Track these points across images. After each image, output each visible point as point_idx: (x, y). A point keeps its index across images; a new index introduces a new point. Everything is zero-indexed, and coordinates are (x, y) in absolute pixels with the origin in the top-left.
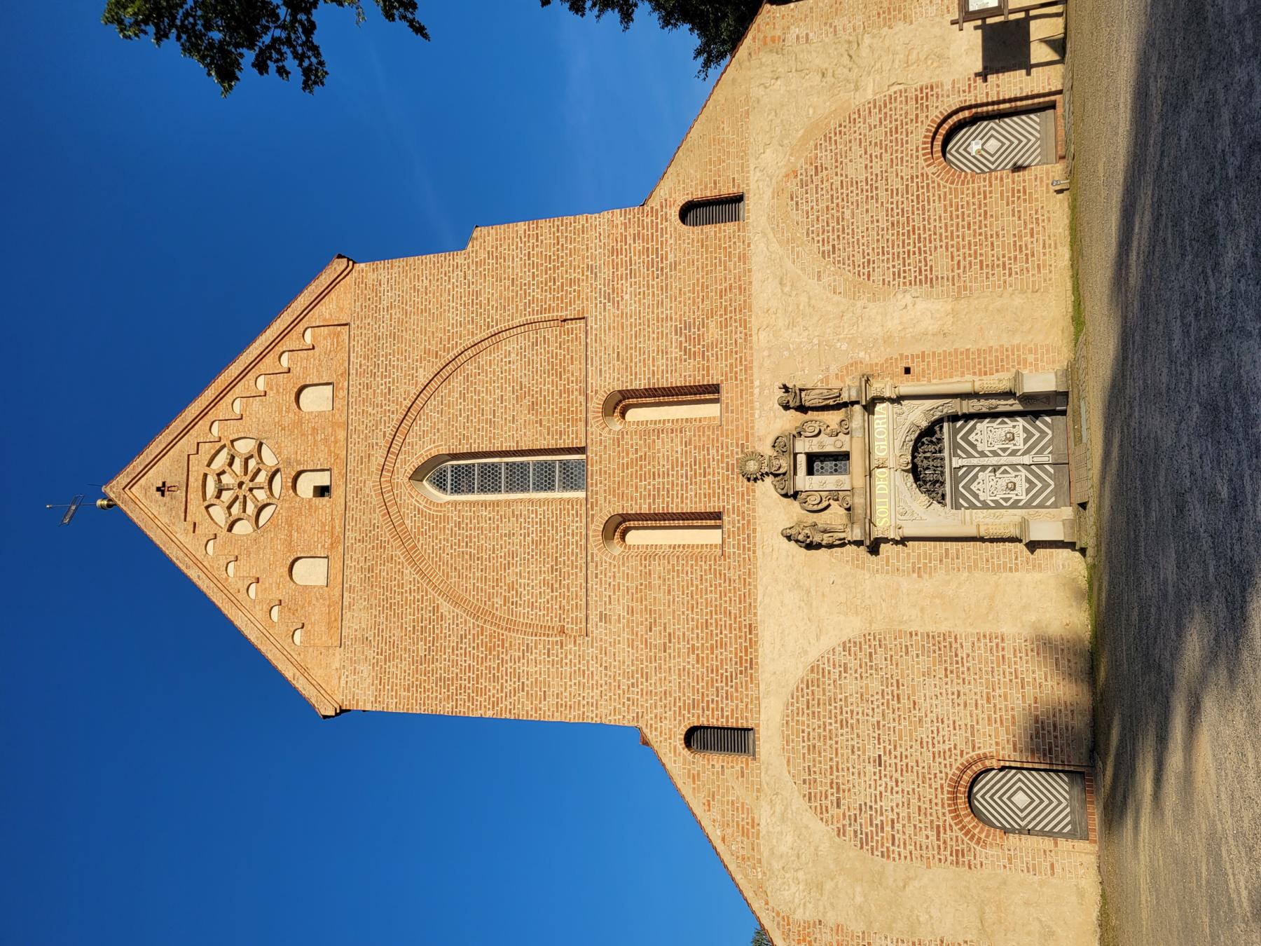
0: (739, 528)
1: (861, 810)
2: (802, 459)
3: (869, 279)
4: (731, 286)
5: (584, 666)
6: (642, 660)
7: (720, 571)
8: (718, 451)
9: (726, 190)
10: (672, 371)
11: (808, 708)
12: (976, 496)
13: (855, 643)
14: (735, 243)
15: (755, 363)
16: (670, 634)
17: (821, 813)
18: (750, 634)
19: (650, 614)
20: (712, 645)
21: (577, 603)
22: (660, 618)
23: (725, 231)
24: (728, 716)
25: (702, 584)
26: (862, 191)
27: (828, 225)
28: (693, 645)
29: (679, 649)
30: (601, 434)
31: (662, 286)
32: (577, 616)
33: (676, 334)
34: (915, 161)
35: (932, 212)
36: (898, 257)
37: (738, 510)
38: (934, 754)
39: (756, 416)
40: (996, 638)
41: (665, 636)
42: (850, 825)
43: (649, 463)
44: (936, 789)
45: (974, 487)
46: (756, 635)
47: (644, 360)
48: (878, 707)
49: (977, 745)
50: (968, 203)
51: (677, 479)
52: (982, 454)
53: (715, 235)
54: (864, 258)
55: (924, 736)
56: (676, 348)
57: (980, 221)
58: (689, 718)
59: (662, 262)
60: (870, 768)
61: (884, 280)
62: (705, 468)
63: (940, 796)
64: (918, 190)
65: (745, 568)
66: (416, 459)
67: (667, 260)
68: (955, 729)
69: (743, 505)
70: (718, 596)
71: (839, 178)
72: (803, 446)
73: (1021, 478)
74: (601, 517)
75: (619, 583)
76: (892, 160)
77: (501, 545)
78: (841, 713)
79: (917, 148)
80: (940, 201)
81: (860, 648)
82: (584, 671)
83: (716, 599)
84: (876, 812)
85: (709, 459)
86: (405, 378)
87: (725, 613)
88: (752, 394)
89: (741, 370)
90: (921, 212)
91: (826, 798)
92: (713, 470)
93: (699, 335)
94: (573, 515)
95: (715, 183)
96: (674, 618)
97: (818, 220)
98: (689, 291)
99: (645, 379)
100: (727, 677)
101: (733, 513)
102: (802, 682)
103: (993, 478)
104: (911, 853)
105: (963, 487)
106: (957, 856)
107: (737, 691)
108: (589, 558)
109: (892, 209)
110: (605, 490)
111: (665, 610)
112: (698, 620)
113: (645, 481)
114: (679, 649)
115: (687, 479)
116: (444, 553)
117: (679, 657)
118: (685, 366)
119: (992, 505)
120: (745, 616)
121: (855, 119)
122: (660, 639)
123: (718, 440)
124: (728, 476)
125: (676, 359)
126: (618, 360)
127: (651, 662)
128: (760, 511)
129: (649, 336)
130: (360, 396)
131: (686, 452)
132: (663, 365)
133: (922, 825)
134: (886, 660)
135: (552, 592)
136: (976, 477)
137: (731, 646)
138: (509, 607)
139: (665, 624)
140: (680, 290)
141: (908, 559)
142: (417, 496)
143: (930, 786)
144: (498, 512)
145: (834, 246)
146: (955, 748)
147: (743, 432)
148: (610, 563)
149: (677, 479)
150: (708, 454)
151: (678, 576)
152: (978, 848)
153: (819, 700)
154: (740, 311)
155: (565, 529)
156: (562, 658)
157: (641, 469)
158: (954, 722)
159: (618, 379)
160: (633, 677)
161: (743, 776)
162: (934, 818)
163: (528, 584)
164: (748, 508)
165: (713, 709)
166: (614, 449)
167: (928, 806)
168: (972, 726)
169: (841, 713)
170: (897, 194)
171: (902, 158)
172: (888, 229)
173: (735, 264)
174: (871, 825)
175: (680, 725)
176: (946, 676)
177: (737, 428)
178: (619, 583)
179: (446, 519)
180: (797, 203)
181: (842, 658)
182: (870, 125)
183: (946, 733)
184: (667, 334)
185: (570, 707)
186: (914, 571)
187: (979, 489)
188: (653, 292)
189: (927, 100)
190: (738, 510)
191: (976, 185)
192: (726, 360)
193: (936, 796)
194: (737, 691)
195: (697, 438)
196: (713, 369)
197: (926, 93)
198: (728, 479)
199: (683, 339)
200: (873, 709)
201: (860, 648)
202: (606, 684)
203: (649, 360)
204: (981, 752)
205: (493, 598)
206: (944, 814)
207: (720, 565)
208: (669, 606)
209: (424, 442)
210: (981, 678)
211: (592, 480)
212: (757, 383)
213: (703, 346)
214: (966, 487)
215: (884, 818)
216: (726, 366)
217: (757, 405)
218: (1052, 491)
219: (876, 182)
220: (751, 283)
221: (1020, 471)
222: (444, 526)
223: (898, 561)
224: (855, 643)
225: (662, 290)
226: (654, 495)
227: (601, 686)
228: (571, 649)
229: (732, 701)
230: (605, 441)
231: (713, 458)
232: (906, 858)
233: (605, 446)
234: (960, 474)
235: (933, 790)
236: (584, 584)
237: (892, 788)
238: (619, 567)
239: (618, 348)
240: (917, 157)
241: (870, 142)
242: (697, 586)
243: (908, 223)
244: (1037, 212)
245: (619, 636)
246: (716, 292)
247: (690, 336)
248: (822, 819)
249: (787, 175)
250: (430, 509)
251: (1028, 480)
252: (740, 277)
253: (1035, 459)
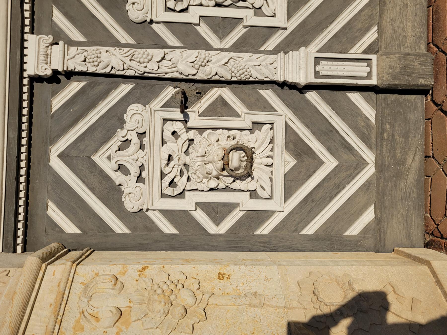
103: (178, 127)
105: (62, 156)
187: (121, 168)
218: (366, 186)
221: (268, 107)
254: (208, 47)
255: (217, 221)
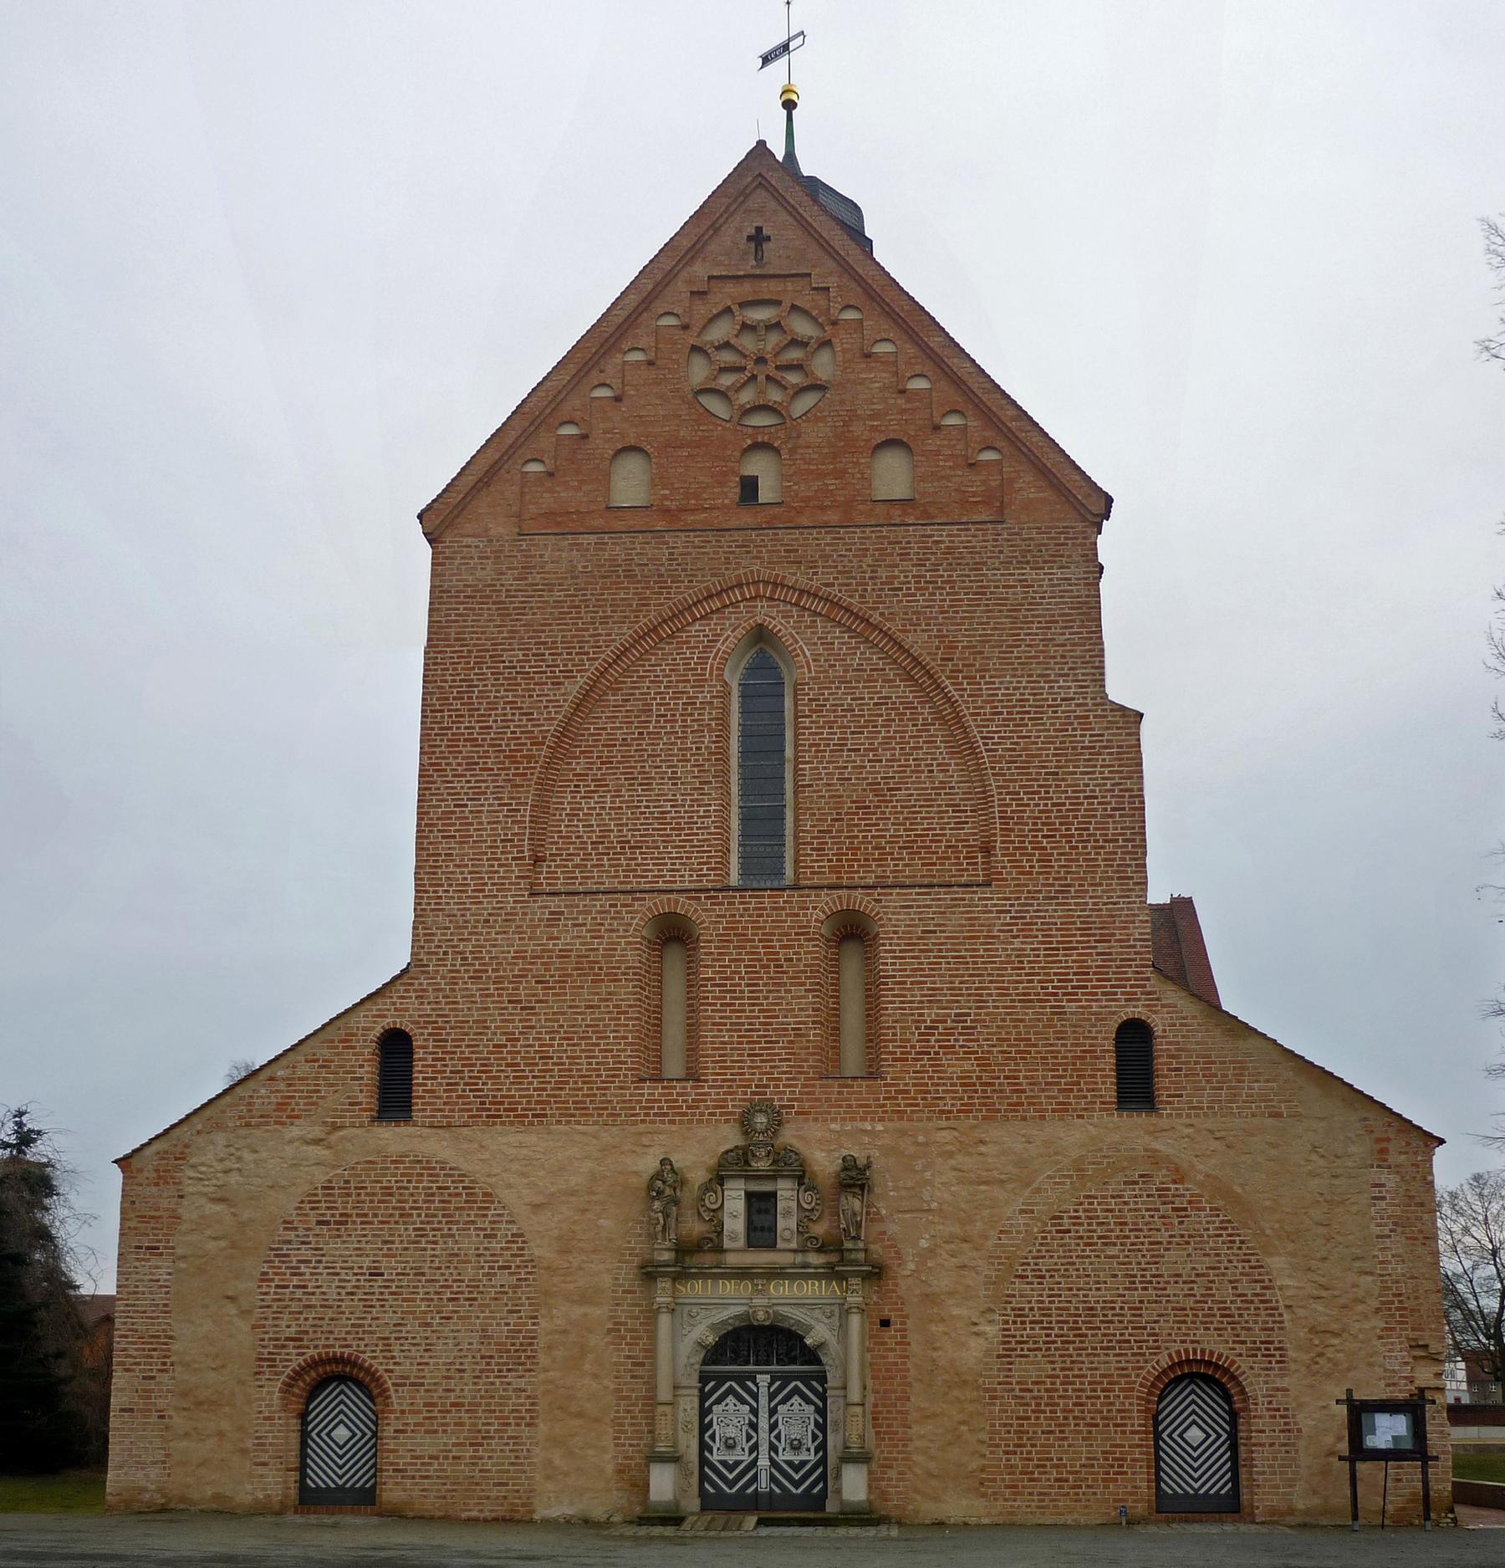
0: (676, 1101)
1: (316, 1249)
2: (766, 1187)
3: (1016, 1276)
4: (1023, 1091)
5: (490, 891)
6: (497, 970)
7: (619, 1076)
8: (785, 1073)
9: (1164, 1084)
10: (904, 1009)
11: (439, 1188)
12: (718, 1401)
13: (522, 1249)
14: (1085, 1097)
15: (905, 1124)
16: (533, 1008)
17: (310, 1202)
18: (534, 1116)
19: (559, 982)
20: (518, 1065)
21: (577, 878)
22: (554, 994)
23: (1104, 1083)
24: (426, 1085)
25: (601, 1051)
26: (1144, 1270)
27: (1099, 1224)
28: (518, 1040)
29: (513, 1021)
30: (815, 908)
31: (1029, 994)
32: (558, 878)
33: (957, 1015)
34: (1178, 1339)
35: (1103, 1358)
36: (1045, 1315)
37: (702, 1101)
38: (388, 1338)
39: (833, 1126)
40: (532, 1418)
41: (530, 1002)
42: (298, 1236)
43: (771, 978)
44: (345, 1339)
45: (731, 1399)
46: (531, 1124)
47: (922, 970)
48: (443, 1274)
49: (400, 1389)
50: (1112, 1404)
51: (747, 1017)
52: (773, 1412)
53: (1099, 1070)
54: (1047, 1271)
55: (409, 1328)
56: (937, 1015)
57: (1084, 1419)
58: (422, 1034)
59: (1065, 994)
60: (367, 1262)
61: (1014, 1296)
62: (762, 1055)
63: (337, 1344)
64: (1136, 1341)
65: (621, 1109)
66: (791, 634)
67: (1069, 1001)
68: (419, 1364)
69: (707, 1107)
70: (584, 1073)
71: (1164, 1240)
72: (786, 1191)
73: (742, 1456)
74: (696, 910)
75: (603, 937)
76: (1185, 1309)
77: (660, 767)
78: (434, 1230)
79: (1198, 1342)
80: (1118, 1369)
81: (516, 1255)
82: (483, 891)
83: (580, 1070)
84: (315, 1268)
85: (774, 1061)
86: (914, 613)
87: (561, 1082)
88: (864, 1119)
89: (899, 1105)
90: (1105, 1344)
91: (328, 1208)
92: (758, 1067)
93: (953, 1047)
94: (701, 870)
95: (1176, 1069)
96: (554, 1013)
97: (1108, 1210)
98: (1019, 1033)
99: (893, 970)
100: (477, 1084)
101: (697, 1094)
102: (472, 1182)
104: (268, 1307)
106: (268, 1360)
107: (459, 1097)
108: (638, 895)
109: (1114, 1308)
110: (734, 916)
111: (565, 1001)
112: (552, 1046)
113: (746, 972)
114: (513, 1021)
115: (747, 1030)
116: (651, 682)
117: (503, 1021)
118: (909, 1028)
119: (707, 1421)
120: (557, 1109)
121: (1249, 1261)
122: (526, 995)
123: (801, 1073)
124: (749, 1086)
125: (921, 1015)
126: (924, 932)
127: (494, 983)
128: (703, 1131)
129: (957, 976)
130: (890, 543)
131: (787, 1030)
132: (912, 996)
133: (301, 1322)
134: (502, 1286)
135: (592, 843)
137: (517, 1090)
138: (572, 781)
139: (546, 1001)
140: (1021, 1021)
141: (632, 1318)
142: (735, 637)
143: (348, 1333)
144: (708, 760)
145: (1069, 1231)
146: (395, 1364)
147: (810, 1107)
148: (630, 925)
149: (747, 1017)
150: (780, 1060)
151: (610, 1019)
152: (279, 1385)
153: (449, 1202)
154: (984, 1105)
155: (682, 858)
156: (500, 859)
157: (762, 966)
158: (427, 1364)
159: (895, 932)
160: (476, 958)
161: (351, 1104)
162: (311, 1336)
163: (604, 808)
164: (702, 1114)
165: (435, 1066)
166: (794, 928)
167: (325, 1329)
168: (422, 1384)
169: (434, 1230)
170: (1134, 1315)
171: (1185, 1322)
172: (1085, 1302)
173: (1053, 1097)
174: (299, 1261)
175: (413, 1022)
176: (482, 1358)
177: (816, 1100)
178: (603, 937)
179: (700, 683)
180: (1136, 1183)
181: (504, 1229)
182: (1237, 1281)
183: (413, 1354)
184: (958, 1001)
185: (434, 873)
186: (616, 1323)
188: (1021, 982)
189: (1263, 1356)
190: (702, 1101)
191: (1135, 1414)
192: (914, 1085)
193: (337, 1340)
194: (459, 1097)
195: (804, 1044)
196: (904, 1066)
197: (1271, 1352)
198: (745, 1086)
199: (949, 1024)
200: (440, 1268)
201: (516, 1255)
202: (466, 922)
203: (921, 976)
204: (392, 1393)
205: (585, 758)
206: (316, 1347)
207: (626, 1076)
208: (570, 1007)
209: (816, 644)
210: (482, 1397)
211: (750, 897)
212: (879, 1127)
213: (937, 1053)
214: (731, 1391)
215: (307, 1277)
216: (906, 1085)
219: (1155, 1288)
220: (1024, 1119)
222: (689, 681)
223: (629, 1305)
224: (522, 1249)
225: (1024, 994)
226: (726, 985)
227: (462, 915)
228: (513, 871)
229: (445, 1091)
230: (805, 915)
231: (775, 1067)
232: (263, 1300)
233: (797, 915)
234: (749, 1383)
235: (343, 1336)
236: (602, 887)
237: (343, 1288)
238: (625, 937)
239: (941, 932)
240: (1183, 1342)
241: (1213, 1282)
242: (598, 1045)
243: (1091, 1328)
244: (1088, 1487)
245: (530, 939)
246: (1015, 1070)
247: (953, 1034)
248: (302, 1202)
249: (1177, 1169)
250: (714, 659)
251: (737, 1463)
252: (1034, 1104)
253: (764, 1472)
254: (770, 1432)
255: (710, 1437)
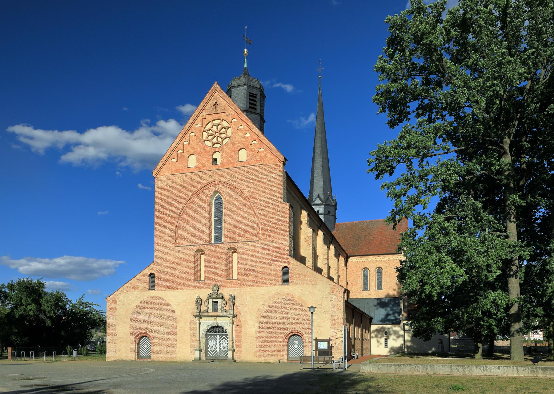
45: (213, 339)
46: (176, 290)
52: (220, 342)
60: (148, 316)
88: (234, 287)
128: (205, 290)
136: (215, 340)
199: (250, 269)
212: (237, 289)
217: (231, 289)
251: (214, 351)
